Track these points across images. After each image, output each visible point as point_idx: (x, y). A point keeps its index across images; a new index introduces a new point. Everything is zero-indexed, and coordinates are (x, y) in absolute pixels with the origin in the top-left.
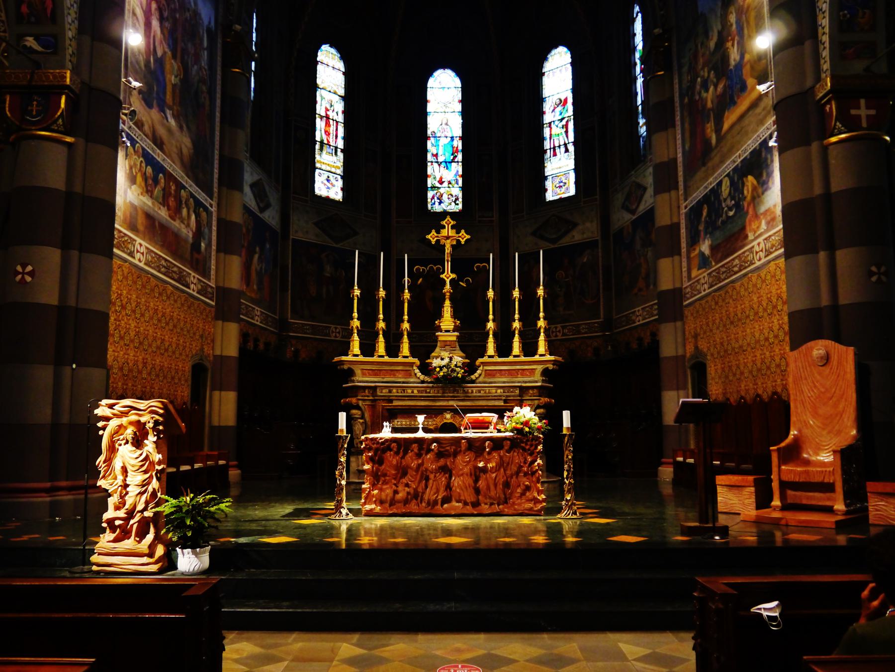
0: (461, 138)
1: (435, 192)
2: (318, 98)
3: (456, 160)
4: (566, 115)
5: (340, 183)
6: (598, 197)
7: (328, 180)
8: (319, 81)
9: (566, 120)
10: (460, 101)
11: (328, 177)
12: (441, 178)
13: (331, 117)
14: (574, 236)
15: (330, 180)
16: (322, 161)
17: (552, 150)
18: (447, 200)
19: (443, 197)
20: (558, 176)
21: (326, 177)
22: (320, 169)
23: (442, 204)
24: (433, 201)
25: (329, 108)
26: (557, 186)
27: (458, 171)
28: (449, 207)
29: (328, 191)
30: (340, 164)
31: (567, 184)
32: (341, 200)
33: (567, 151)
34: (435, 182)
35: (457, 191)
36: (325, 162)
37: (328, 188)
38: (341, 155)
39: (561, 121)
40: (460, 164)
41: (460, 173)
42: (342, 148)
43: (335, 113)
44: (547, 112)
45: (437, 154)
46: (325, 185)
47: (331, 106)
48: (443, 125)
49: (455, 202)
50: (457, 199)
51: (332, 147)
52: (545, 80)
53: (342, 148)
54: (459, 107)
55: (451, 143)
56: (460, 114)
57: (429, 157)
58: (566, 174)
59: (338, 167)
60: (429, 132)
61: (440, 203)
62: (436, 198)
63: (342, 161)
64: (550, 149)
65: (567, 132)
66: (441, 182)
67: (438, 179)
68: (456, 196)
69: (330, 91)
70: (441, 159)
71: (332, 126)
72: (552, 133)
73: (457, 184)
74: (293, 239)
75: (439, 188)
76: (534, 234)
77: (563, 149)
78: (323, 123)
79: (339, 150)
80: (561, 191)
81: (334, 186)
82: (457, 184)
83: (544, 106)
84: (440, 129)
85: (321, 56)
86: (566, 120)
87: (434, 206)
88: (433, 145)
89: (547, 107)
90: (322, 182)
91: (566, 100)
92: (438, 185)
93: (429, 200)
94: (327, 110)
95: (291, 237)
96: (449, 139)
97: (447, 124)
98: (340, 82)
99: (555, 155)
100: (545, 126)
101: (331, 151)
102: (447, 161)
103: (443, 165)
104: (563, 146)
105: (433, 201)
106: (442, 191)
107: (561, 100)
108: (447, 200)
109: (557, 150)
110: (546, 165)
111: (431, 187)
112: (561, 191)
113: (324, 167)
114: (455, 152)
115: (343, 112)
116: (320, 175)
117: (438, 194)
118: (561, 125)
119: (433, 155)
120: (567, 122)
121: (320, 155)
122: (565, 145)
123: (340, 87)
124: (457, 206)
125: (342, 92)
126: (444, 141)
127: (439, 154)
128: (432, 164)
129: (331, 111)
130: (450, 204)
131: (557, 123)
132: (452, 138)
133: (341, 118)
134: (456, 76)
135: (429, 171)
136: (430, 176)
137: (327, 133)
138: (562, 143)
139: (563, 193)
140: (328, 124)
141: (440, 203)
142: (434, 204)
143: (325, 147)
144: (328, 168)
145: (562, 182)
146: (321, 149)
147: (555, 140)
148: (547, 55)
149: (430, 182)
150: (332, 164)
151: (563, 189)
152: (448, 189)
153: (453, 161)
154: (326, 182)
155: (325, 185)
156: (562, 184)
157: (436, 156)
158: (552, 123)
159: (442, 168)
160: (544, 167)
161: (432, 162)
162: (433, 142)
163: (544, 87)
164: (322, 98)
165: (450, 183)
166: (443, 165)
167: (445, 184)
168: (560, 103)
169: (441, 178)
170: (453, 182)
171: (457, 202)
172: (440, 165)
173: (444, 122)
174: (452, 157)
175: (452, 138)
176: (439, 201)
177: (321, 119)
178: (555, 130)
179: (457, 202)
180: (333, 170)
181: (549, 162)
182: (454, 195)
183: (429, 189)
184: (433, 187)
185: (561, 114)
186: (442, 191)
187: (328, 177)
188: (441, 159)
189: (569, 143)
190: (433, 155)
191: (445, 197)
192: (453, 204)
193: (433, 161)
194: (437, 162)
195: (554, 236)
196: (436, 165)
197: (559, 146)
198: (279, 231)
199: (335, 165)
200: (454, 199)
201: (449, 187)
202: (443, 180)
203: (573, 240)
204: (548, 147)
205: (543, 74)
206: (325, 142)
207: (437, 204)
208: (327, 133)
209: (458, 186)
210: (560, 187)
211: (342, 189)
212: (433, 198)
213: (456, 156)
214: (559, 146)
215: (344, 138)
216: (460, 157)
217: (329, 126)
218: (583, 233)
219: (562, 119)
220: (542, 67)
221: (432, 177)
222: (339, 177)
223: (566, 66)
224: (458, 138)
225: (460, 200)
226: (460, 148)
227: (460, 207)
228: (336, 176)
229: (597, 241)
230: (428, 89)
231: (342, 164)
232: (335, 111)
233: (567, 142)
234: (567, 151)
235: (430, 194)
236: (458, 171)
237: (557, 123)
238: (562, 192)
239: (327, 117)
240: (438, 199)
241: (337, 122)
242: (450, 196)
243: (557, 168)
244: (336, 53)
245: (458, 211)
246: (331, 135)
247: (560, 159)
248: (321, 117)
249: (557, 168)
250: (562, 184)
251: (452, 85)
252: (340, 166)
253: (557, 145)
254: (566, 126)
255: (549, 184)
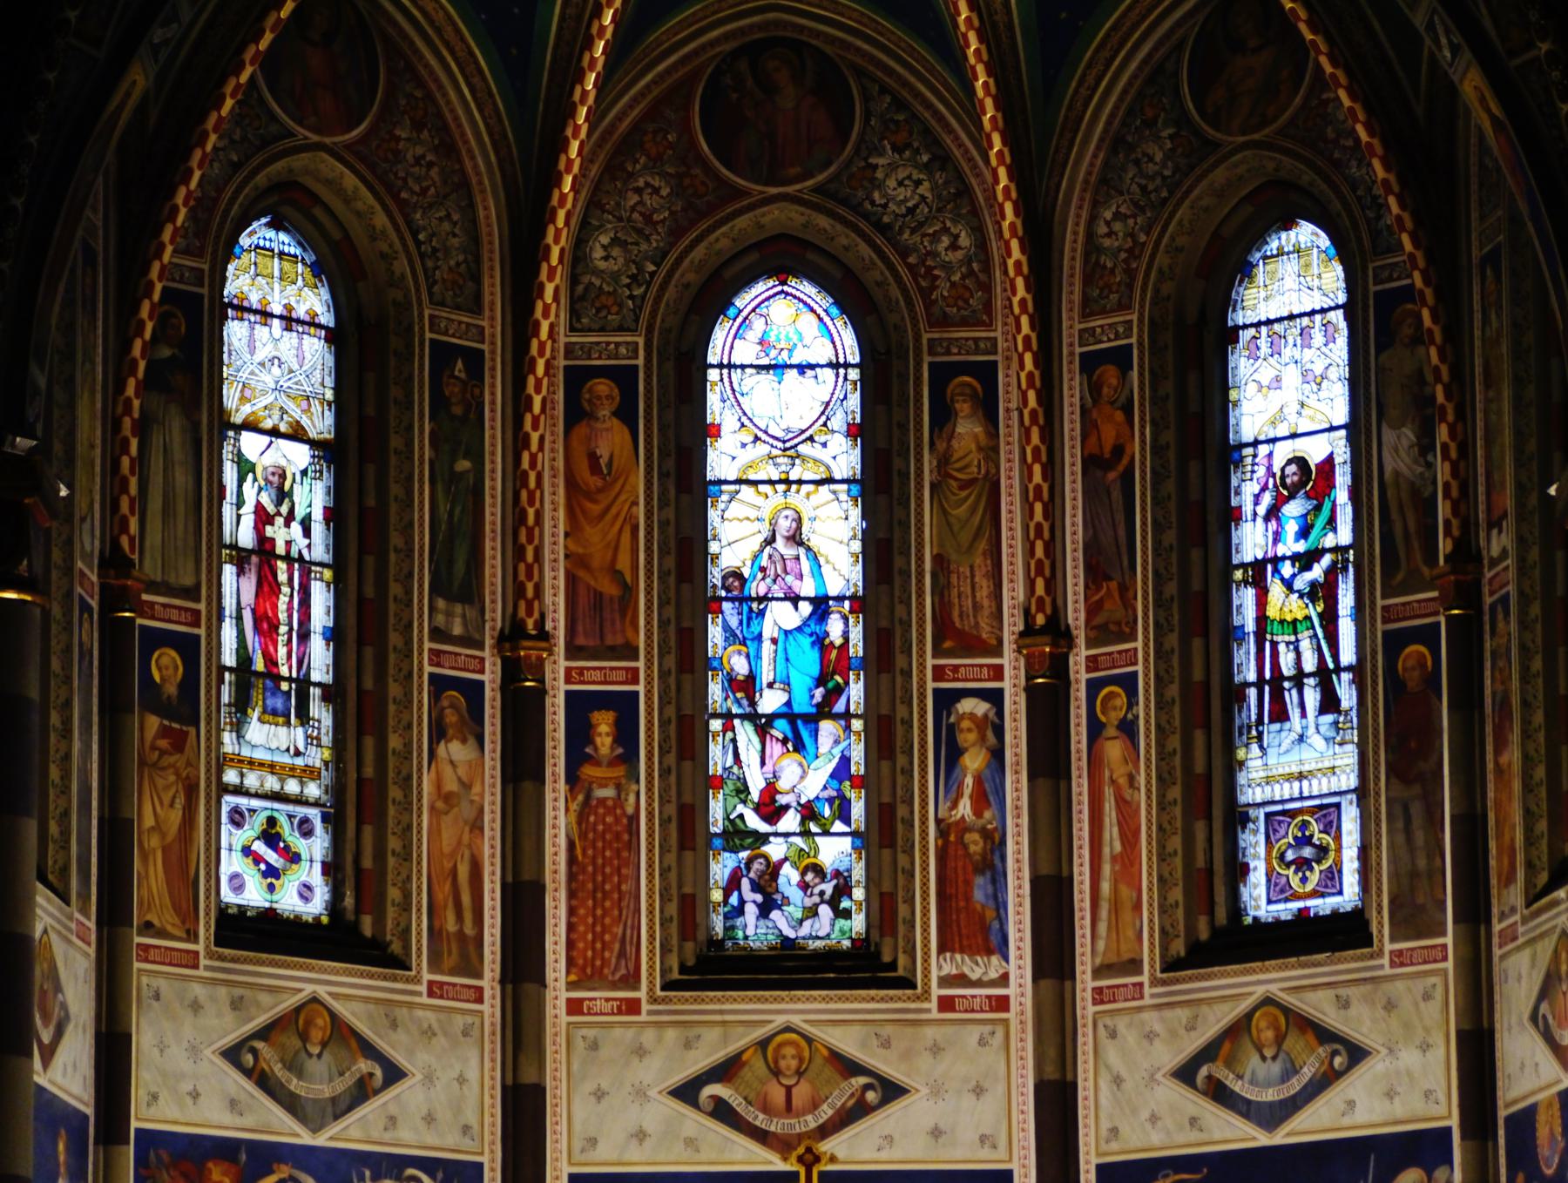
0: (859, 604)
1: (744, 855)
2: (230, 474)
3: (840, 707)
4: (1329, 541)
5: (316, 847)
6: (1449, 940)
7: (270, 836)
8: (230, 397)
9: (1327, 560)
10: (853, 432)
11: (272, 821)
12: (770, 790)
13: (280, 549)
14: (1351, 1104)
15: (278, 837)
16: (246, 752)
17: (1267, 688)
18: (795, 894)
19: (782, 880)
20: (1292, 814)
21: (259, 821)
22: (239, 790)
23: (775, 915)
24: (734, 900)
25: (271, 509)
26: (1290, 855)
27: (845, 761)
28: (805, 930)
29: (271, 888)
30: (316, 757)
31: (1332, 854)
32: (325, 920)
33: (1330, 703)
34: (740, 808)
35: (834, 850)
36: (259, 755)
37: (272, 872)
38: (321, 712)
39: (1307, 567)
40: (857, 725)
41: (858, 767)
42: (328, 679)
43: (296, 528)
44: (1248, 509)
45: (751, 678)
46: (258, 859)
47: (282, 495)
48: (780, 544)
49: (833, 903)
50: (843, 889)
51: (284, 686)
52: (1241, 365)
53: (328, 679)
54: (844, 458)
55: (813, 627)
56: (855, 489)
57: (715, 690)
58: (1328, 813)
59: (309, 773)
60: (715, 576)
61: (764, 910)
62: (745, 884)
63: (326, 740)
64: (1260, 683)
65: (1330, 619)
66: (770, 809)
67: (755, 795)
68: (837, 874)
69: (274, 433)
70: (770, 702)
71: (285, 590)
72: (1272, 612)
73: (845, 818)
74: (138, 1131)
75: (763, 838)
76: (1185, 1074)
77: (1312, 697)
78: (249, 587)
79: (315, 692)
80: (1304, 880)
81: (295, 858)
82: (847, 820)
83: (1234, 482)
84: (764, 562)
85: (239, 282)
86: (1327, 560)
87: (739, 921)
88: (731, 636)
89: (1248, 491)
90: (247, 851)
91: (1328, 464)
92: (754, 822)
93: (717, 895)
94: (263, 518)
95: (134, 1124)
96: (806, 608)
97: (796, 538)
98: (317, 376)
99: (1280, 715)
100: (1238, 575)
101: (279, 703)
102: (797, 709)
103: (782, 726)
104: (1311, 681)
105: (734, 900)
106: (775, 850)
107: (1301, 462)
108: (795, 894)
109: (1291, 698)
110: (1241, 754)
111: (725, 834)
112: (1304, 880)
113: (252, 780)
114: (832, 667)
115: (330, 515)
116: (238, 817)
117: (757, 866)
118: (1301, 583)
119: (733, 683)
120: (1331, 573)
121: (238, 728)
122: (1325, 677)
123: (316, 407)
124: (841, 923)
125: (321, 424)
126: (782, 616)
127: (766, 675)
128: (728, 727)
129: (280, 521)
130: (812, 912)
131: (1287, 569)
132: (821, 605)
133: (319, 547)
134: (834, 311)
135: (718, 758)
136: (717, 783)
137: (266, 625)
138: (1310, 664)
139: (1315, 894)
140: (267, 587)
141: (764, 910)
142: (740, 910)
143: (257, 696)
144: (272, 783)
145: (1305, 841)
146: (242, 704)
147: (1282, 648)
148: (1249, 251)
149: (717, 809)
150: (286, 759)
151: (1314, 878)
152: (798, 841)
153: (824, 711)
154: (260, 847)
155: (258, 859)
156: (1307, 852)
157: (747, 686)
158: (1269, 567)
159: (775, 749)
160: (1233, 766)
161: (728, 717)
162: (734, 622)
163: (1233, 395)
164: (245, 468)
165: (809, 812)
166: (782, 726)
167: (790, 822)
168: (1302, 484)
169: (770, 790)
170: (827, 812)
171: (845, 904)
172: (763, 726)
173: (785, 525)
174: (821, 690)
175: (821, 605)
176: (759, 898)
177: (241, 572)
178: (1281, 603)
179: (845, 904)
180: (292, 787)
181: (1255, 747)
182: (829, 871)
183: (718, 842)
184: (737, 835)
185: (1304, 533)
186: (775, 850)
187: (272, 821)
188: (770, 702)
189: (1338, 669)
190: (733, 683)
191: (789, 875)
192: (825, 911)
193: (735, 710)
194: (752, 717)
195: (1270, 1095)
196: (745, 733)
197: (1299, 678)
198: (89, 1111)
199: (299, 761)
200: (828, 888)
201: (806, 833)
202: (782, 800)
203: (1346, 1121)
204: (1252, 676)
205: (1232, 335)
206: (259, 665)
207: (751, 911)
208: (266, 625)
209: (846, 829)
210: (1302, 864)
211: (327, 869)
212: (733, 884)
213: (838, 691)
214: (1299, 678)
215: (334, 636)
216: (856, 691)
217: (276, 589)
218: (1390, 1095)
219: (1305, 561)
220: (1227, 303)
221: (730, 786)
222: (314, 814)
223: (1332, 315)
224: (847, 604)
225: (859, 893)
226: (857, 648)
227: (858, 923)
228: (301, 811)
229: (1448, 1130)
230: (713, 374)
231: (327, 754)
232: (300, 512)
233: (1331, 666)
234: (1330, 703)
235: (722, 867)
236: (845, 761)
237: (1287, 569)
238: (1309, 887)
239: (264, 546)
240: (756, 887)
241: (306, 566)
242: (809, 877)
243: (1289, 778)
244: (298, 251)
245: (846, 943)
246: (283, 629)
247: (1301, 738)
248: (241, 558)
249: (1289, 778)
250: (1307, 852)
251: (821, 352)
252: (318, 764)
253: (1287, 668)
254: (1324, 592)
255: (1254, 844)
